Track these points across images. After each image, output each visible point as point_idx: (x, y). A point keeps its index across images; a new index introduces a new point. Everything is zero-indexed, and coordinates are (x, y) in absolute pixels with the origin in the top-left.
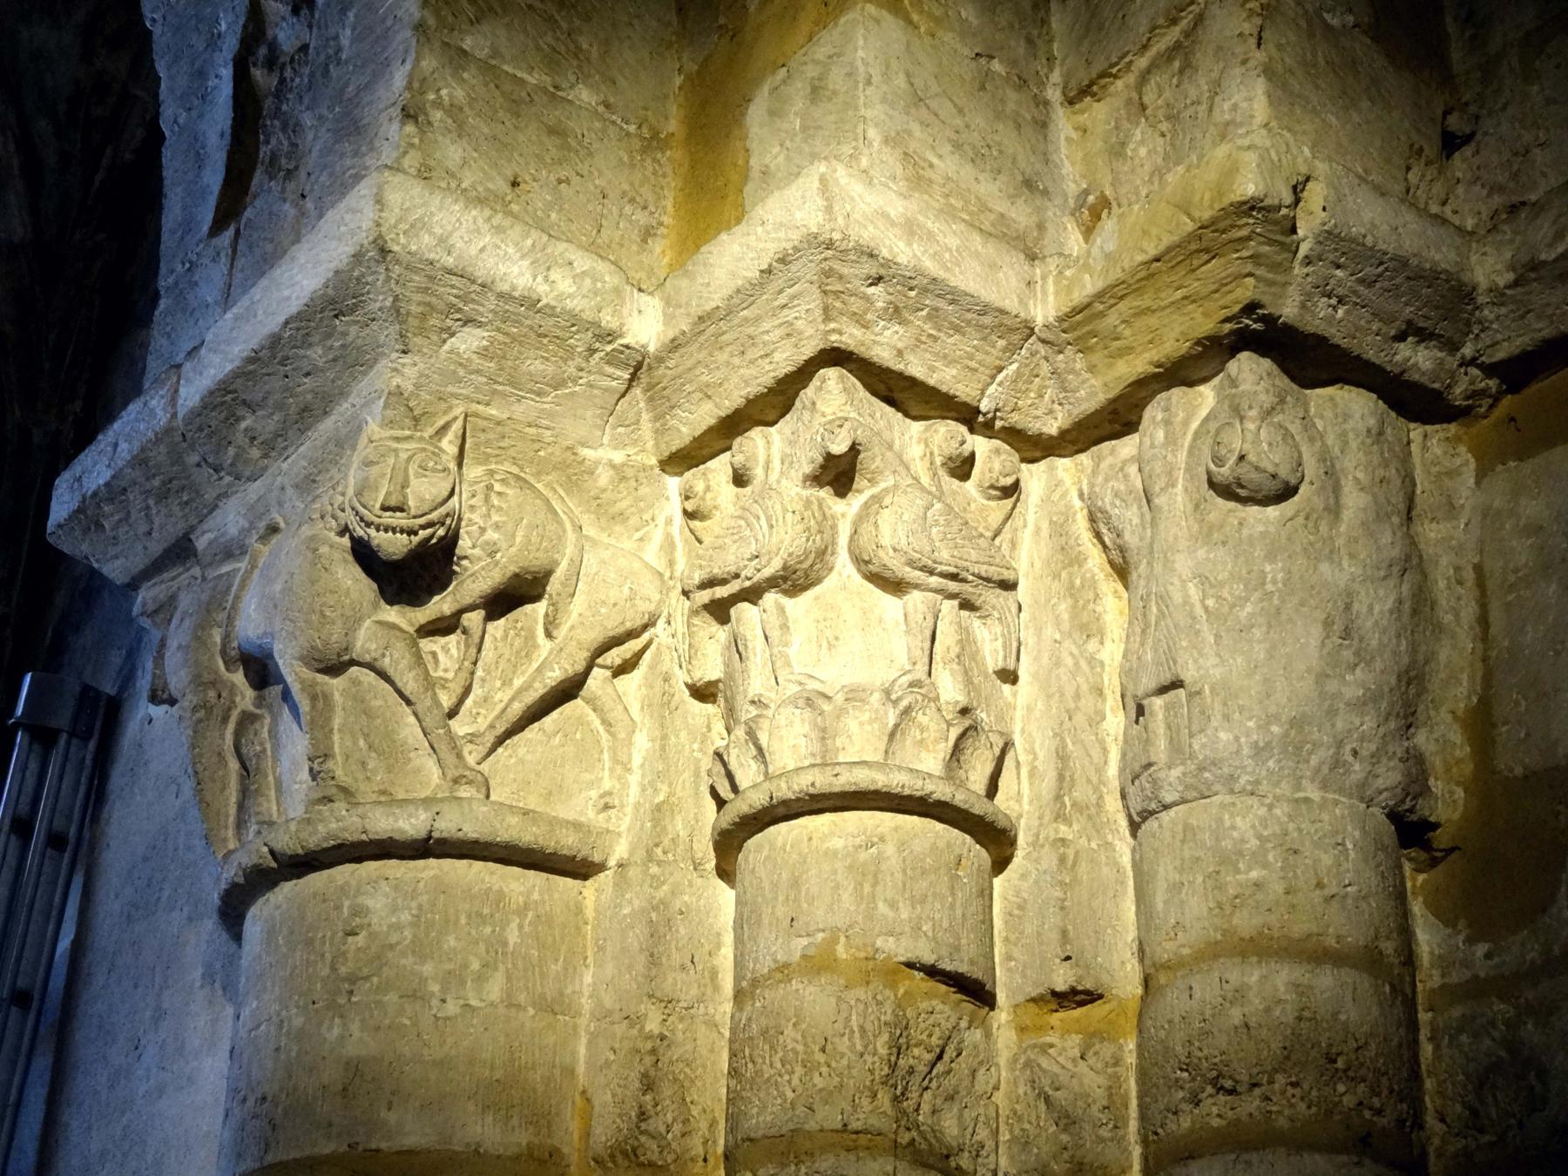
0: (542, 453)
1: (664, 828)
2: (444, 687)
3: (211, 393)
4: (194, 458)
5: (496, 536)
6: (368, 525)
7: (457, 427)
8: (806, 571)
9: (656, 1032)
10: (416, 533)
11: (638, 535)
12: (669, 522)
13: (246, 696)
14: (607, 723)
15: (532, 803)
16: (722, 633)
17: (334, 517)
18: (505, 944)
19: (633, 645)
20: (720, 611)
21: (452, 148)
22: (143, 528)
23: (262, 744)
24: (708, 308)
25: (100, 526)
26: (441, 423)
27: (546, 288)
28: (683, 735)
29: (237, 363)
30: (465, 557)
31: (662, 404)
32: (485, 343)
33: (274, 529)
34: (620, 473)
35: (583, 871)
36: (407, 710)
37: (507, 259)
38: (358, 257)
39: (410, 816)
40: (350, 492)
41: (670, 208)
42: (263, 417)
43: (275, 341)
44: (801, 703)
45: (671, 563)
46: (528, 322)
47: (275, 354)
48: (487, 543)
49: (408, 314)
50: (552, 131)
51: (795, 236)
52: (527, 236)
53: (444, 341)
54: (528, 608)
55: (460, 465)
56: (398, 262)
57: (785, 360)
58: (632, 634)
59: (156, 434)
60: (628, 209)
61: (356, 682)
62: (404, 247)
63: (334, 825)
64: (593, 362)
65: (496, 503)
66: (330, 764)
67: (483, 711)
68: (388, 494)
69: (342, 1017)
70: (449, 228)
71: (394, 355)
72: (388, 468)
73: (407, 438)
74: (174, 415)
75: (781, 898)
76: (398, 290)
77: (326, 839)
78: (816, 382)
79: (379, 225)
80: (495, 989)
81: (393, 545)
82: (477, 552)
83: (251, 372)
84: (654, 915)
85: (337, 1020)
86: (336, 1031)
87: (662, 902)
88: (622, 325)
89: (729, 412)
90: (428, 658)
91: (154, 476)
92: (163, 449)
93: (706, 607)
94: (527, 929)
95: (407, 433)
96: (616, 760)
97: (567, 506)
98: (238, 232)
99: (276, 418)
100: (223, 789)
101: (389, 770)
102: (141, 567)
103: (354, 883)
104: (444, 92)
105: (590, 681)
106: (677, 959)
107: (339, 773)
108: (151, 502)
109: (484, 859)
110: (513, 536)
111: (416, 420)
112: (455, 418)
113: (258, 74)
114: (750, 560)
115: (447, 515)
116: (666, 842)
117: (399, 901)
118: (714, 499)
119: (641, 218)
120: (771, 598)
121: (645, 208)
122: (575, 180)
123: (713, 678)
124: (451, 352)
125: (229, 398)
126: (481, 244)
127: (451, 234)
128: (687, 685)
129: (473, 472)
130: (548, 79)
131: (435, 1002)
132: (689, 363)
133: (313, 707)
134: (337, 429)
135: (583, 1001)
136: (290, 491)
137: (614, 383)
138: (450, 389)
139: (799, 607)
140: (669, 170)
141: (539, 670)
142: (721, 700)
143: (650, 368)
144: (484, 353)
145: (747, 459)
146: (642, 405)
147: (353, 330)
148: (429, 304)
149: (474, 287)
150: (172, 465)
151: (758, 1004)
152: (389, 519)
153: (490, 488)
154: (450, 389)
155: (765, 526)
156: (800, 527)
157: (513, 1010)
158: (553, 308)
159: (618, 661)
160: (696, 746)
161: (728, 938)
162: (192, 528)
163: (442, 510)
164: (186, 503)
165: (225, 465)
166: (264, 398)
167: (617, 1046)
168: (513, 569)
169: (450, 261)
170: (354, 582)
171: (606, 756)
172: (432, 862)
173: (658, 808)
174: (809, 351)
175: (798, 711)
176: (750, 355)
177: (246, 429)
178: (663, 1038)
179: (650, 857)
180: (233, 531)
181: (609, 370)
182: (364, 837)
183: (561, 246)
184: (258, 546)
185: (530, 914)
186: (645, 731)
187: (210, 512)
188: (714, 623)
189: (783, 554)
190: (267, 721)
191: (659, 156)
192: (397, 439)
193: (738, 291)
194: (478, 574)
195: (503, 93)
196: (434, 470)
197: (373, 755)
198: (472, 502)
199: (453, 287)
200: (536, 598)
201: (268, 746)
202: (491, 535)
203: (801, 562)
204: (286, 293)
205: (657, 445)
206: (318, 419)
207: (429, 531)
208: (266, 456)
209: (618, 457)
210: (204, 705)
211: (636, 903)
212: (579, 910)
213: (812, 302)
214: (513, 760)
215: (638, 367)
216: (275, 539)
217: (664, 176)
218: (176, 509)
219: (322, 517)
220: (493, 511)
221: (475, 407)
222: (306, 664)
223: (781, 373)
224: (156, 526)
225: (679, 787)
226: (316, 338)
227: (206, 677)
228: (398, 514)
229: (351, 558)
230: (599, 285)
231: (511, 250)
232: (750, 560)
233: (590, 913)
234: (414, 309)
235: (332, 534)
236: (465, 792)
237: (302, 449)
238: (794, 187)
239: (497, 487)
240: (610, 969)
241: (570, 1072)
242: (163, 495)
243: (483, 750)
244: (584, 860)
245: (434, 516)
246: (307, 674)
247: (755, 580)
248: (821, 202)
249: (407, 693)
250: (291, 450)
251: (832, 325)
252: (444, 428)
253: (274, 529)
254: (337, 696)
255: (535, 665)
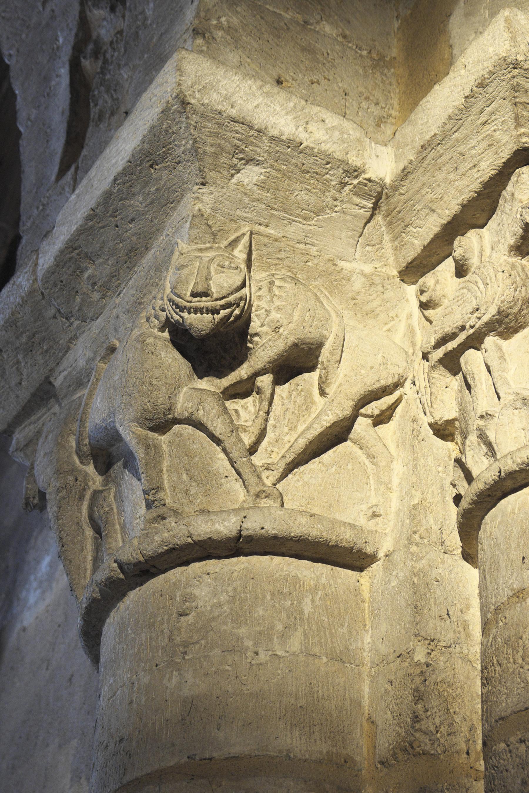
0: (310, 264)
1: (419, 521)
2: (245, 431)
3: (62, 252)
4: (51, 312)
5: (279, 316)
6: (182, 309)
7: (246, 238)
8: (516, 315)
9: (423, 661)
10: (218, 313)
11: (386, 328)
12: (410, 316)
13: (96, 480)
14: (371, 457)
15: (316, 510)
16: (456, 382)
17: (157, 317)
18: (302, 612)
19: (387, 401)
20: (451, 363)
21: (232, 55)
23: (109, 505)
24: (428, 137)
26: (232, 238)
27: (306, 135)
28: (430, 459)
29: (80, 223)
30: (256, 334)
31: (398, 225)
32: (262, 177)
33: (112, 350)
34: (370, 281)
35: (358, 564)
36: (218, 449)
37: (277, 113)
38: (165, 112)
39: (224, 520)
40: (168, 291)
41: (396, 106)
42: (101, 264)
43: (107, 196)
44: (519, 404)
45: (413, 344)
46: (294, 161)
47: (109, 206)
48: (272, 321)
49: (205, 152)
50: (304, 49)
51: (489, 65)
52: (290, 100)
53: (232, 176)
54: (306, 376)
55: (249, 268)
56: (195, 112)
57: (487, 168)
58: (386, 391)
59: (22, 298)
60: (364, 104)
61: (178, 435)
62: (198, 101)
63: (166, 535)
64: (344, 194)
65: (277, 293)
66: (161, 495)
67: (276, 449)
68: (196, 284)
69: (179, 670)
70: (232, 90)
71: (196, 188)
72: (196, 269)
73: (207, 249)
74: (36, 279)
75: (513, 546)
76: (196, 134)
77: (160, 546)
78: (513, 178)
79: (179, 85)
80: (295, 644)
81: (201, 322)
82: (265, 329)
83: (91, 228)
84: (416, 580)
85: (175, 673)
86: (175, 681)
87: (421, 570)
88: (364, 164)
89: (449, 219)
90: (233, 413)
91: (22, 333)
92: (28, 309)
93: (441, 361)
94: (318, 603)
95: (208, 245)
96: (379, 482)
97: (332, 304)
98: (77, 168)
99: (110, 263)
100: (82, 550)
101: (207, 494)
102: (14, 413)
103: (183, 579)
104: (223, 19)
105: (356, 426)
106: (436, 611)
107: (169, 501)
108: (20, 357)
109: (283, 555)
110: (291, 315)
111: (214, 235)
112: (244, 235)
113: (87, 64)
114: (472, 313)
115: (241, 299)
116: (422, 530)
117: (219, 588)
118: (443, 290)
119: (375, 110)
120: (490, 341)
121: (377, 104)
122: (323, 82)
123: (450, 418)
124: (238, 184)
125: (74, 254)
126: (256, 103)
127: (233, 95)
128: (430, 425)
129: (258, 275)
130: (299, 17)
131: (250, 654)
132: (416, 188)
133: (147, 454)
134: (156, 258)
135: (365, 654)
136: (123, 317)
137: (362, 211)
138: (238, 212)
139: (510, 346)
140: (394, 82)
141: (317, 417)
142: (458, 438)
143: (388, 197)
144: (262, 185)
145: (465, 252)
146: (383, 228)
147: (164, 175)
148: (219, 146)
149: (252, 132)
150: (35, 322)
151: (501, 624)
152: (197, 303)
153: (271, 283)
154: (238, 212)
155: (481, 286)
156: (509, 281)
157: (311, 658)
158: (312, 149)
159: (377, 412)
160: (440, 469)
161: (476, 602)
162: (52, 370)
163: (238, 295)
164: (47, 351)
165: (74, 312)
166: (101, 247)
167: (392, 678)
168: (292, 339)
169: (233, 112)
170: (174, 362)
171: (371, 481)
172: (242, 558)
173: (414, 507)
174: (506, 154)
175: (517, 411)
176: (462, 169)
177: (88, 278)
178: (428, 665)
179: (410, 541)
180: (82, 363)
181: (357, 200)
182: (189, 540)
183: (316, 109)
184: (101, 365)
185: (320, 593)
186: (400, 461)
187: (64, 355)
188: (448, 375)
189: (497, 302)
190: (113, 490)
191: (386, 71)
192: (201, 250)
193: (450, 118)
194: (265, 349)
195: (267, 22)
196: (230, 268)
197: (194, 484)
198: (260, 293)
199: (237, 132)
200: (311, 369)
201: (114, 507)
202: (275, 315)
203: (511, 308)
204: (114, 161)
205: (397, 260)
206: (142, 255)
207: (228, 310)
208: (104, 296)
209: (368, 268)
210: (65, 486)
211: (401, 575)
212: (358, 593)
213: (506, 114)
214: (300, 484)
215: (378, 198)
216: (112, 356)
217: (390, 84)
218: (40, 360)
219: (148, 319)
220: (275, 299)
221: (257, 228)
222: (141, 424)
223: (485, 178)
224: (25, 376)
225: (429, 495)
226: (137, 188)
227: (66, 468)
228: (204, 299)
229: (170, 345)
230: (346, 136)
231: (278, 108)
232: (472, 313)
233: (366, 595)
234: (209, 149)
235: (156, 330)
236: (264, 503)
237: (130, 283)
238: (486, 34)
239: (277, 283)
240: (384, 627)
241: (359, 704)
242: (29, 349)
243: (277, 474)
244: (360, 551)
245: (232, 298)
246: (141, 431)
247: (477, 326)
248: (507, 35)
249: (217, 434)
250: (123, 286)
251: (523, 130)
252: (235, 242)
253: (112, 350)
254: (164, 447)
255: (313, 416)
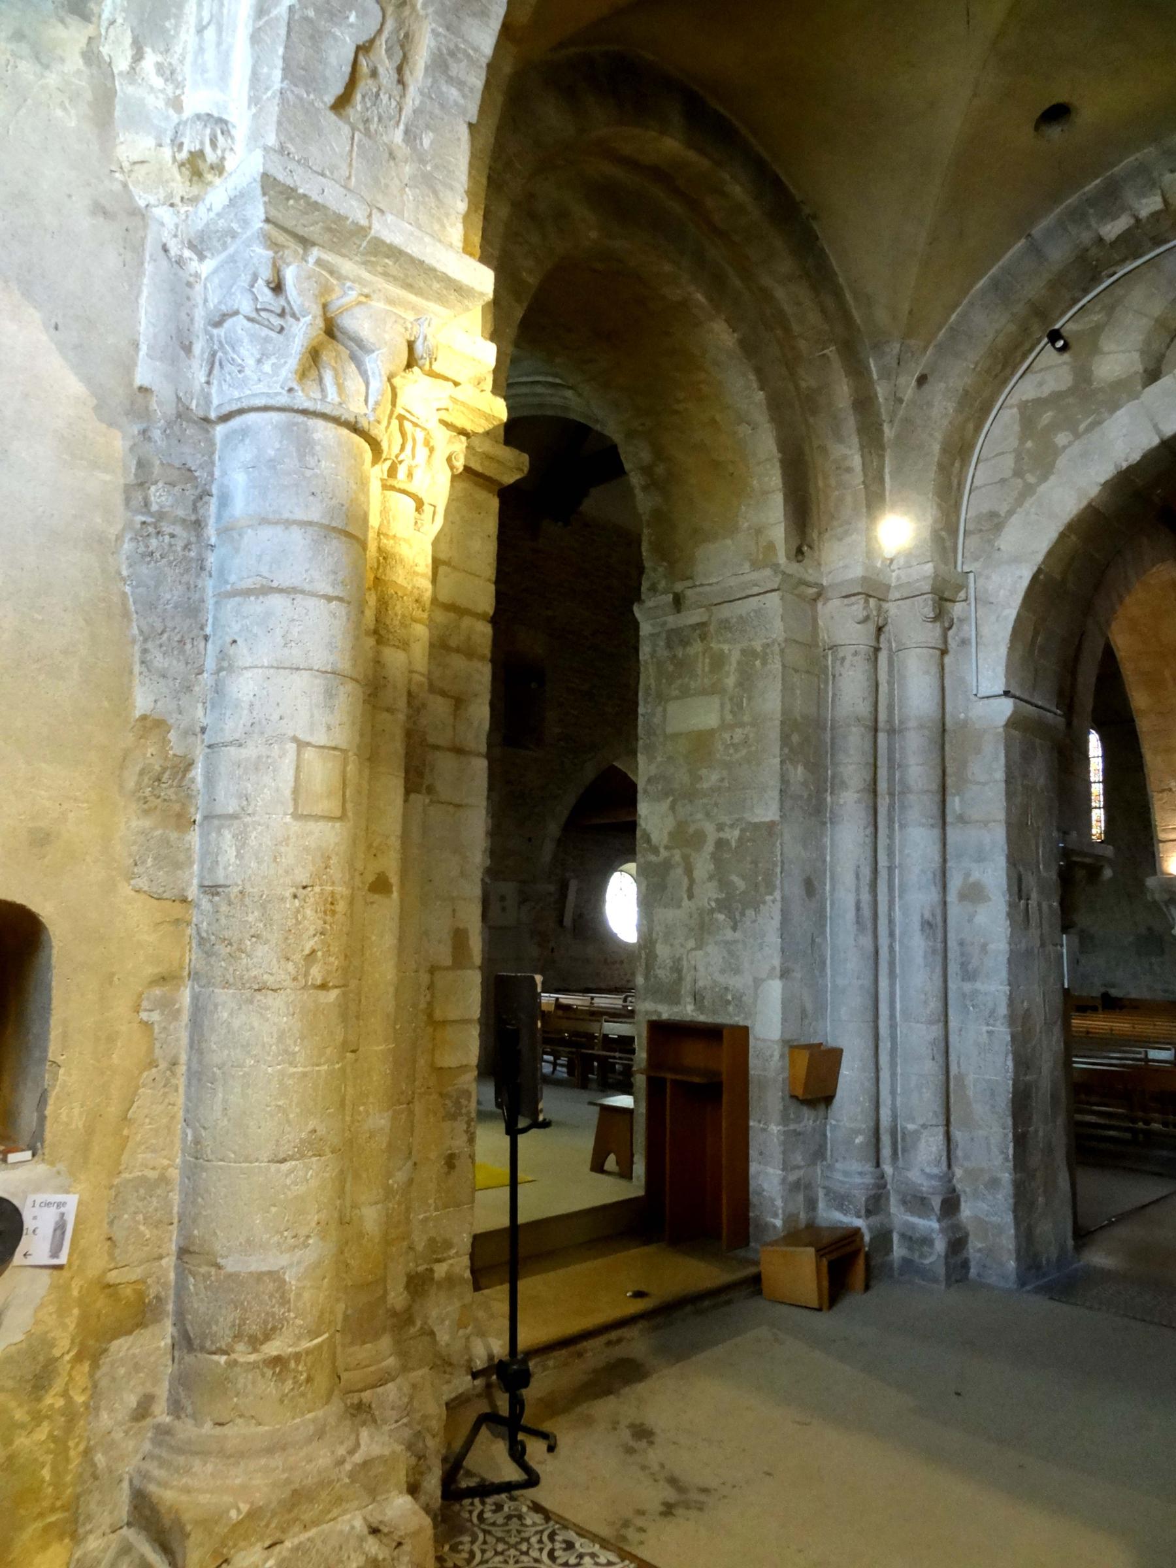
3: (396, 247)
22: (305, 222)
25: (288, 199)
43: (434, 270)
92: (353, 227)
180: (343, 272)
